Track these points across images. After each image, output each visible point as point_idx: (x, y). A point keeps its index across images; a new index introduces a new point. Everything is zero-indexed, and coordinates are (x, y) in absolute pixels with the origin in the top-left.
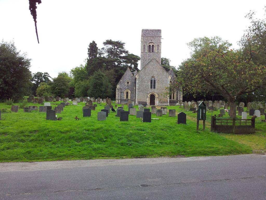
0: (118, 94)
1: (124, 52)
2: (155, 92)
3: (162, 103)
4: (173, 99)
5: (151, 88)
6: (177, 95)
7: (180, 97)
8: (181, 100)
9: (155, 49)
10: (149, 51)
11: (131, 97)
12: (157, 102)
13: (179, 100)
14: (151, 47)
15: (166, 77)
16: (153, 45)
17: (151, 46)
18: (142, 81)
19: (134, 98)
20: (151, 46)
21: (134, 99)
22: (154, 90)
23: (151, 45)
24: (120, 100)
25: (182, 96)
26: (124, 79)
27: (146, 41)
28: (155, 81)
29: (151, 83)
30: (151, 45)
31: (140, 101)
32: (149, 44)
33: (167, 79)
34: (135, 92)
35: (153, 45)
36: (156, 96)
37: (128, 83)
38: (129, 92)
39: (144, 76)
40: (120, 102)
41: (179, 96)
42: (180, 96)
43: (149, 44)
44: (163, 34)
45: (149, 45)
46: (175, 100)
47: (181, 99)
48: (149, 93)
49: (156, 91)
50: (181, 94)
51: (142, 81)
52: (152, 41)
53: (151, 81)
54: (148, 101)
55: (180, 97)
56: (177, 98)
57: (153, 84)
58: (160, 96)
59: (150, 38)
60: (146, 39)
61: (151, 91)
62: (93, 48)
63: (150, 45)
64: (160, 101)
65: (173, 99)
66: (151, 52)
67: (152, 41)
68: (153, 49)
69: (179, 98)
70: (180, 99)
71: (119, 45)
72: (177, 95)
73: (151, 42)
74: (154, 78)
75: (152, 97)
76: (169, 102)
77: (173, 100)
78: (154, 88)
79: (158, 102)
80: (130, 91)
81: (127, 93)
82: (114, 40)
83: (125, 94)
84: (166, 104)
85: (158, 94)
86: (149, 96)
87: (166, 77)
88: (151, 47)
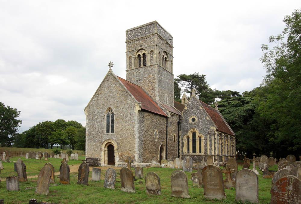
4: (200, 152)
5: (108, 131)
6: (206, 145)
14: (142, 59)
16: (144, 54)
17: (141, 56)
20: (141, 56)
30: (141, 53)
33: (132, 111)
35: (144, 54)
36: (116, 147)
39: (97, 110)
45: (137, 55)
49: (114, 137)
52: (141, 46)
55: (211, 149)
56: (206, 150)
58: (120, 148)
59: (138, 42)
62: (239, 92)
63: (139, 55)
65: (200, 152)
67: (141, 46)
68: (145, 62)
69: (208, 150)
70: (211, 153)
72: (206, 145)
73: (141, 48)
78: (113, 131)
85: (118, 143)
88: (142, 59)
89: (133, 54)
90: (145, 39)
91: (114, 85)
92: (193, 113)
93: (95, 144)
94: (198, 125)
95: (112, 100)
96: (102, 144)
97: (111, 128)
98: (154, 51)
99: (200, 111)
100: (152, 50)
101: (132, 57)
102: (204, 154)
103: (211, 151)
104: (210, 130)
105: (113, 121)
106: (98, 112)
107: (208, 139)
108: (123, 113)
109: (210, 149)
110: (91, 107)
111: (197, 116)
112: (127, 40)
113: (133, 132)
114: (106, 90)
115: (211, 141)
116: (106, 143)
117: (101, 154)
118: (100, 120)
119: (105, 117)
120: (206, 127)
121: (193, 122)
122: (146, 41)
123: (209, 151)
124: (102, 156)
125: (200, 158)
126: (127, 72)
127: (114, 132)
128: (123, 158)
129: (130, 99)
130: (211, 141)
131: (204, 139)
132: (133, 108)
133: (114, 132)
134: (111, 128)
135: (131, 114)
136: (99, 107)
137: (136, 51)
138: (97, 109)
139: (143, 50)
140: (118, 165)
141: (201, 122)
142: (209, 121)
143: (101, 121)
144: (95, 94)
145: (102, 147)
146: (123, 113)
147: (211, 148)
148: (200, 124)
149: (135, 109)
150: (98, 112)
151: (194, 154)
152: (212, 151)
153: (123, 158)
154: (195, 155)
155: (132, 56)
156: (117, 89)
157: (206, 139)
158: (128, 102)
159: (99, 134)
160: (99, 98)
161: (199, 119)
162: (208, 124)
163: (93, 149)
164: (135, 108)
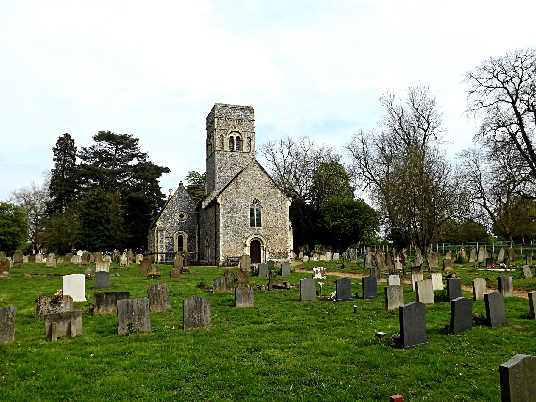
1: (137, 156)
2: (262, 232)
3: (275, 257)
5: (252, 225)
9: (246, 143)
10: (232, 149)
11: (189, 248)
15: (282, 202)
16: (238, 138)
17: (235, 138)
18: (232, 210)
19: (197, 248)
20: (235, 138)
21: (197, 251)
23: (235, 136)
24: (165, 255)
26: (172, 208)
29: (252, 214)
30: (235, 136)
31: (228, 255)
32: (232, 135)
33: (283, 206)
34: (197, 237)
37: (181, 216)
38: (185, 235)
39: (237, 200)
40: (166, 260)
43: (232, 135)
44: (256, 116)
51: (232, 210)
53: (252, 210)
57: (255, 218)
60: (225, 123)
61: (251, 233)
63: (232, 137)
66: (235, 150)
71: (126, 142)
73: (235, 130)
75: (256, 246)
78: (259, 225)
80: (185, 234)
81: (180, 238)
82: (118, 131)
83: (176, 242)
84: (284, 260)
85: (267, 238)
86: (248, 243)
87: (282, 202)
95: (257, 191)
100: (249, 136)
101: (224, 136)
105: (259, 215)
116: (251, 238)
127: (260, 226)
132: (283, 203)
133: (260, 226)
143: (244, 213)
150: (238, 202)
155: (224, 135)
156: (263, 180)
159: (241, 228)
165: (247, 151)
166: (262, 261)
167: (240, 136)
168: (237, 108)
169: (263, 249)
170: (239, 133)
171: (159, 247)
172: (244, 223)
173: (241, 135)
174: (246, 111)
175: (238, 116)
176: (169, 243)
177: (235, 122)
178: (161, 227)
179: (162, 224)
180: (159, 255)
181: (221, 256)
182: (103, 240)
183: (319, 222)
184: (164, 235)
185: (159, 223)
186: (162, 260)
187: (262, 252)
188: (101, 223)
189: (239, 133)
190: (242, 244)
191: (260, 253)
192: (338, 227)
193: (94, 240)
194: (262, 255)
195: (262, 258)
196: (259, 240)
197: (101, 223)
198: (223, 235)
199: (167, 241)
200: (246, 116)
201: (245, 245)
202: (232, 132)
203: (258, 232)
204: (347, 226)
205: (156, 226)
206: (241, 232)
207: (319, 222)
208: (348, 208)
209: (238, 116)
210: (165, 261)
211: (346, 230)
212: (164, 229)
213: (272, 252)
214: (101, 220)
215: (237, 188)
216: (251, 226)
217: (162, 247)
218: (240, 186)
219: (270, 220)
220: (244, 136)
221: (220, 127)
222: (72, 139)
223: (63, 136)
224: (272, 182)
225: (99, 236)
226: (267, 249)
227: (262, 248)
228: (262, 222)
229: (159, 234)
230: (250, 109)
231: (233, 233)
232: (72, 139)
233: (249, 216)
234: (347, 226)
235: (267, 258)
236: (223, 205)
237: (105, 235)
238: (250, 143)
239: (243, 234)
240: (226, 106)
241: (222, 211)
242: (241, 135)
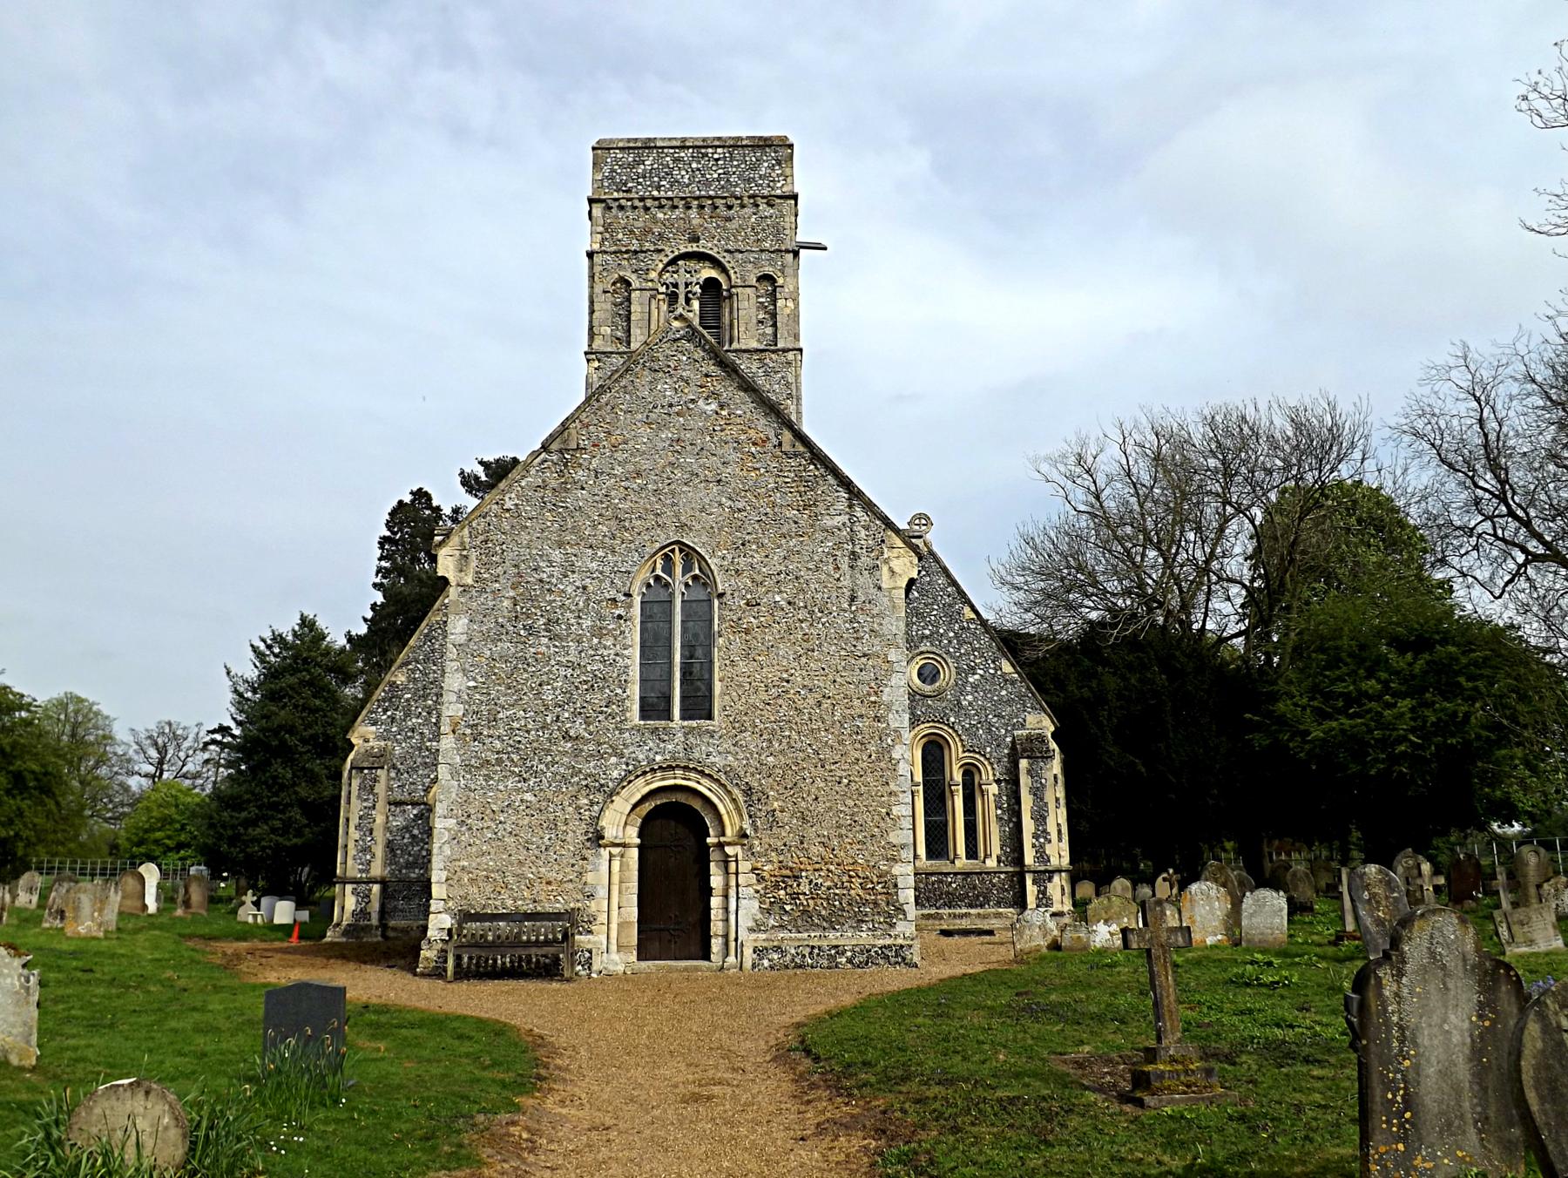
0: (354, 821)
2: (713, 755)
3: (806, 918)
4: (972, 853)
5: (654, 707)
7: (1041, 834)
8: (1054, 861)
9: (746, 306)
12: (738, 908)
13: (1029, 859)
15: (854, 556)
18: (531, 616)
22: (689, 732)
24: (376, 888)
25: (1058, 818)
27: (635, 246)
28: (699, 615)
29: (654, 645)
31: (479, 899)
33: (864, 580)
39: (557, 555)
41: (1028, 826)
42: (1040, 818)
46: (991, 863)
47: (1059, 853)
48: (624, 781)
50: (1049, 797)
51: (531, 616)
52: (696, 239)
54: (612, 896)
55: (1041, 834)
58: (773, 821)
60: (642, 220)
64: (785, 896)
69: (1028, 841)
70: (1042, 856)
74: (687, 568)
75: (677, 846)
76: (908, 895)
77: (962, 863)
78: (699, 705)
79: (749, 909)
84: (864, 937)
85: (748, 791)
86: (620, 822)
87: (854, 556)
89: (641, 272)
90: (722, 211)
91: (714, 406)
92: (924, 637)
93: (528, 797)
94: (959, 702)
96: (600, 797)
97: (682, 686)
98: (780, 281)
99: (963, 628)
100: (768, 270)
101: (635, 284)
102: (999, 861)
103: (1042, 846)
104: (1025, 732)
106: (569, 569)
107: (1025, 781)
108: (789, 589)
109: (1036, 836)
110: (506, 526)
111: (948, 653)
112: (598, 185)
113: (878, 719)
114: (645, 431)
115: (1038, 793)
116: (640, 788)
117: (589, 878)
118: (587, 623)
119: (630, 606)
120: (999, 716)
121: (927, 688)
122: (729, 219)
123: (1034, 846)
124: (603, 893)
125: (975, 888)
126: (596, 364)
127: (710, 717)
128: (794, 896)
129: (842, 505)
130: (1038, 793)
131: (998, 782)
132: (865, 561)
133: (710, 717)
134: (682, 686)
135: (853, 599)
136: (575, 530)
137: (666, 260)
138: (560, 545)
139: (707, 264)
140: (759, 952)
141: (975, 687)
142: (1013, 683)
143: (599, 632)
144: (545, 448)
145: (603, 823)
146: (789, 589)
147: (1045, 831)
148: (970, 698)
149: (885, 569)
150: (569, 569)
151: (941, 865)
152: (1047, 846)
153: (794, 896)
154: (947, 874)
155: (632, 278)
156: (733, 431)
157: (1011, 782)
158: (828, 522)
159: (578, 728)
160: (580, 475)
161: (959, 671)
162: (1009, 702)
163: (509, 840)
164: (886, 561)
165: (754, 345)
166: (716, 945)
167: (721, 278)
168: (701, 147)
169: (725, 862)
170: (716, 263)
171: (352, 852)
172: (597, 698)
173: (724, 270)
174: (751, 158)
175: (708, 184)
176: (407, 828)
177: (693, 213)
178: (368, 754)
179: (379, 737)
180: (349, 888)
181: (435, 905)
182: (288, 825)
183: (1256, 727)
184: (380, 788)
185: (364, 736)
186: (362, 913)
187: (716, 881)
188: (286, 753)
189: (716, 263)
190: (576, 834)
191: (708, 891)
192: (1356, 745)
193: (248, 823)
194: (715, 902)
195: (716, 927)
196: (697, 805)
197: (286, 753)
198: (454, 774)
199: (398, 822)
200: (749, 180)
201: (597, 838)
202: (673, 262)
203: (688, 749)
204: (1404, 739)
205: (352, 746)
206: (577, 753)
207: (1256, 727)
208: (1400, 645)
209: (708, 184)
210: (375, 921)
211: (1394, 759)
212: (378, 760)
213: (781, 891)
214: (283, 742)
215: (563, 488)
216: (645, 713)
217: (366, 850)
218: (580, 475)
219: (771, 674)
220: (742, 273)
221: (616, 242)
222: (435, 503)
223: (407, 499)
224: (787, 436)
225: (274, 806)
226: (745, 866)
227: (714, 855)
228: (718, 687)
229: (355, 783)
230: (777, 149)
231: (522, 761)
232: (435, 503)
233: (636, 652)
234: (1404, 739)
235: (746, 922)
236: (465, 589)
237: (302, 803)
238: (774, 302)
239: (590, 767)
240: (648, 145)
241: (458, 627)
242: (724, 270)
